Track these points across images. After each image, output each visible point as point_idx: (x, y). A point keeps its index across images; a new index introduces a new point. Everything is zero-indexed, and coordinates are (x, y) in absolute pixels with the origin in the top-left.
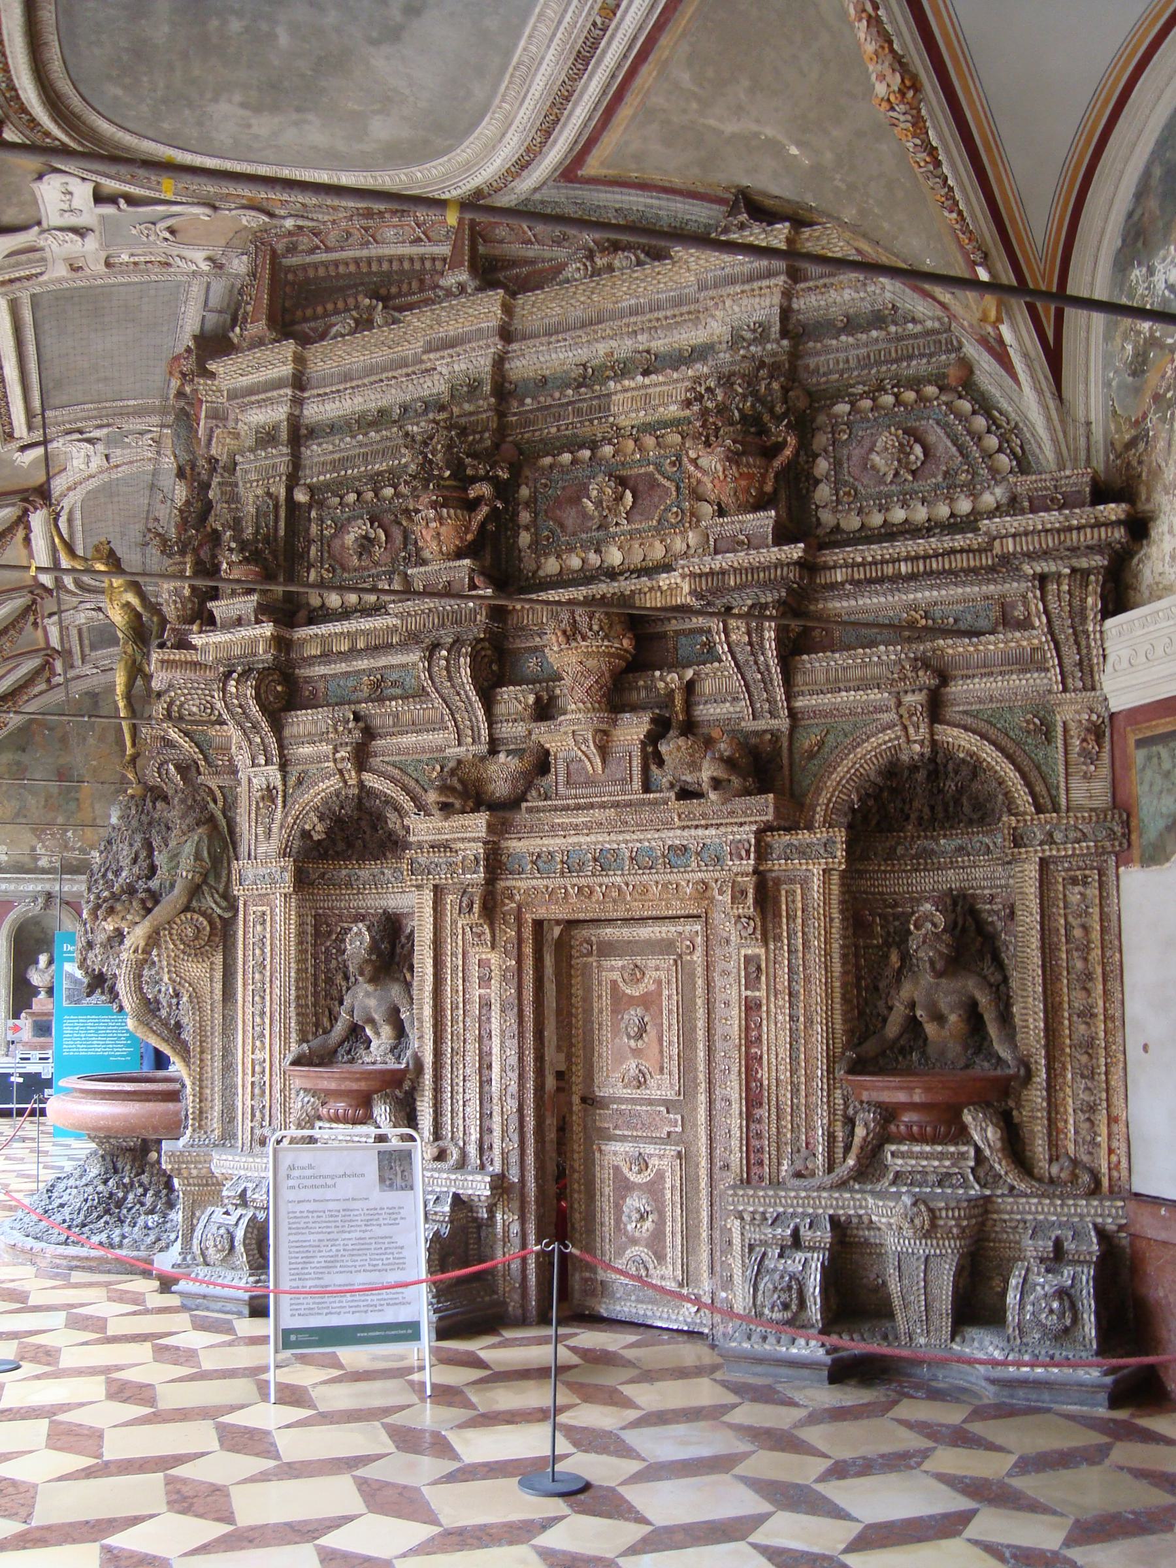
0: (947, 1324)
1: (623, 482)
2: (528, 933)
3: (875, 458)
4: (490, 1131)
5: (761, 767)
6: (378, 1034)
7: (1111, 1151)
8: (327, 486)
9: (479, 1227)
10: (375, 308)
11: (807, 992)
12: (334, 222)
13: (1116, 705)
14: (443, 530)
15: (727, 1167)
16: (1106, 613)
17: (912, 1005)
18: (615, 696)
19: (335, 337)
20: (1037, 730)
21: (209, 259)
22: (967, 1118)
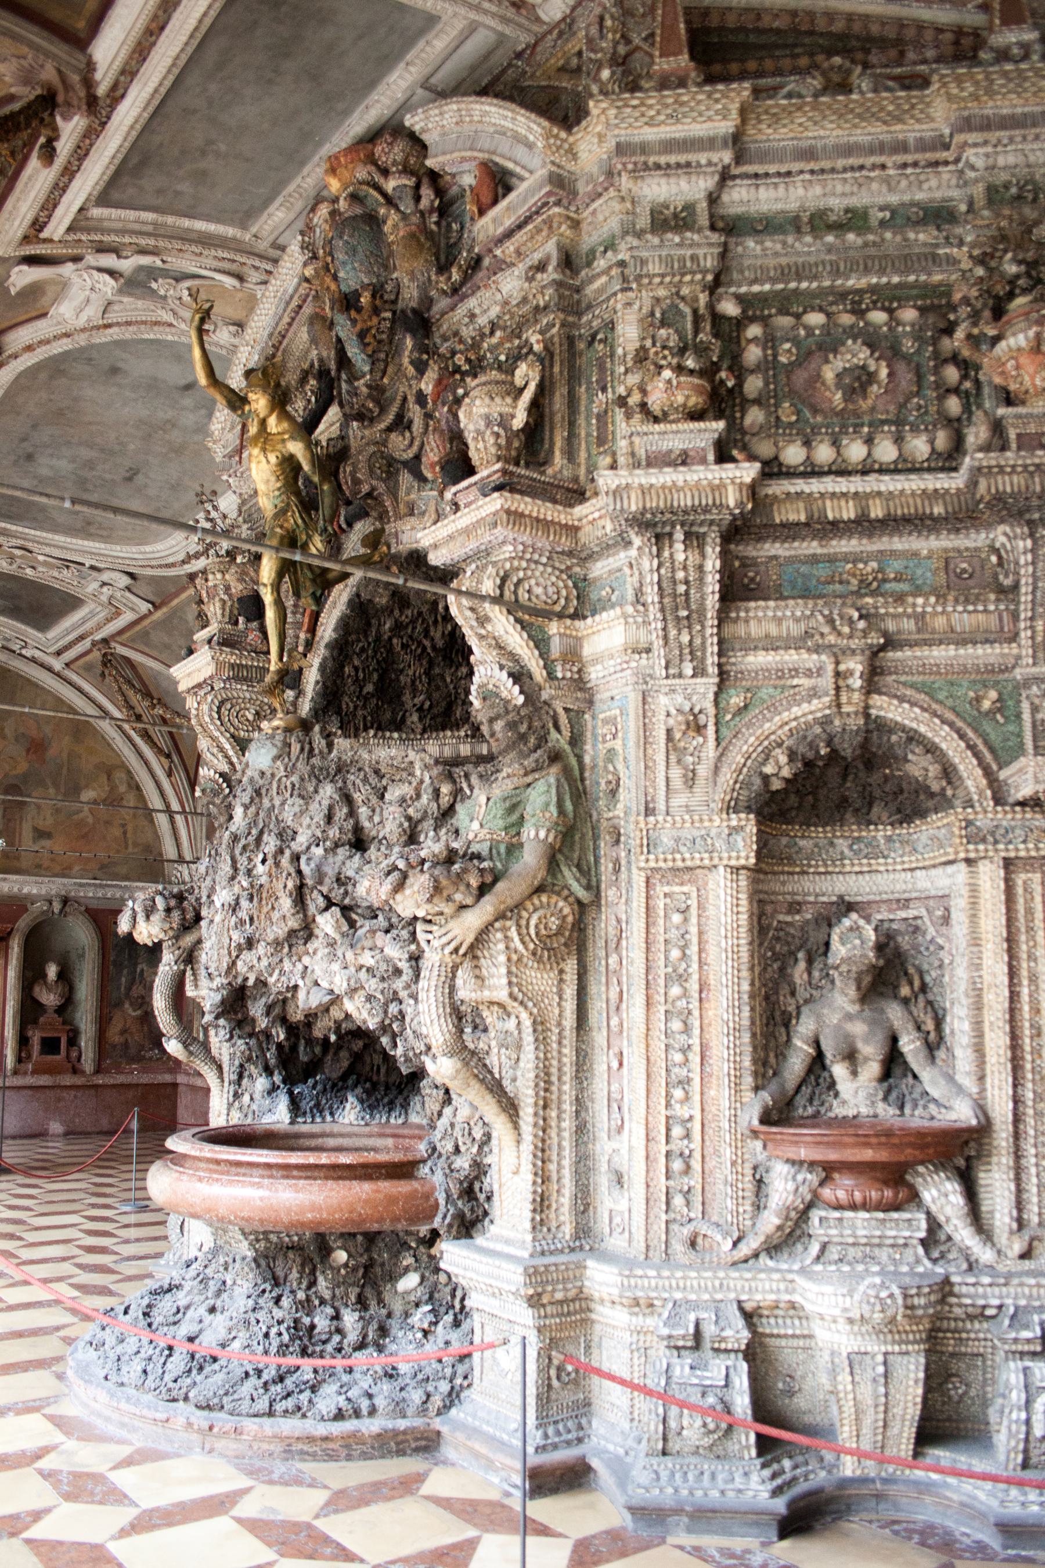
6: (854, 1073)
8: (763, 299)
10: (849, 72)
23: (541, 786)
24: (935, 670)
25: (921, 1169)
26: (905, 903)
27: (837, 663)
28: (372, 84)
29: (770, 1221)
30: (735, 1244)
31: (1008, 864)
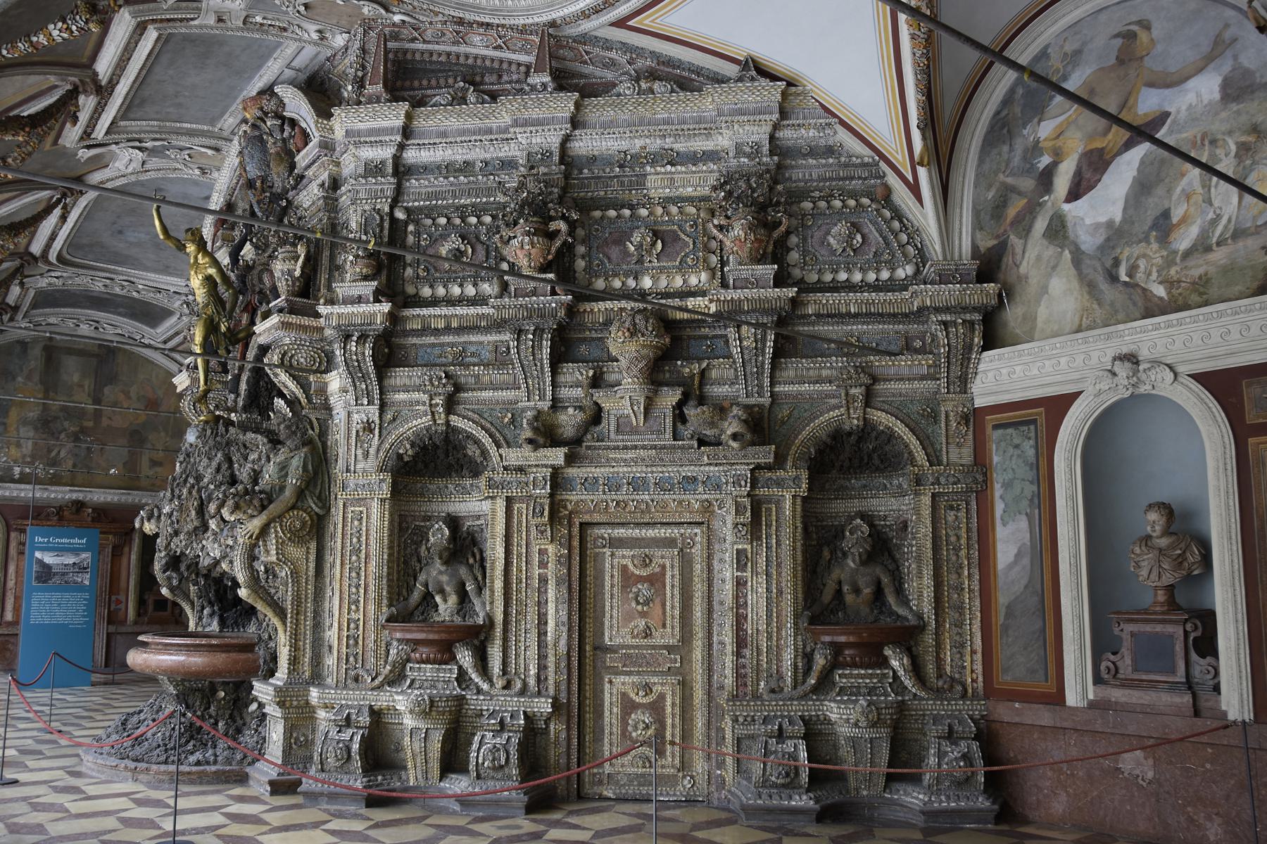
0: (882, 781)
1: (656, 234)
2: (576, 530)
3: (831, 240)
4: (546, 667)
5: (760, 426)
6: (445, 601)
7: (972, 671)
8: (420, 209)
9: (535, 735)
11: (779, 574)
12: (431, 23)
13: (979, 403)
14: (533, 251)
15: (722, 688)
16: (986, 347)
17: (840, 583)
18: (656, 372)
19: (434, 105)
20: (929, 415)
21: (319, 31)
22: (888, 652)
23: (297, 458)
24: (484, 402)
26: (478, 517)
27: (431, 399)
28: (260, 67)
30: (373, 680)
31: (509, 500)
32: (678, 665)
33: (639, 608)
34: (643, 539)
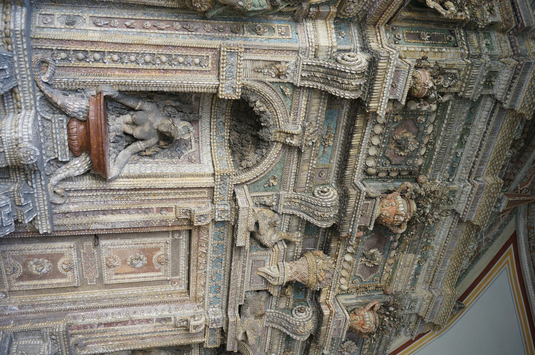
15: (75, 318)
25: (88, 159)
29: (59, 99)
32: (89, 283)
33: (129, 260)
34: (178, 258)
